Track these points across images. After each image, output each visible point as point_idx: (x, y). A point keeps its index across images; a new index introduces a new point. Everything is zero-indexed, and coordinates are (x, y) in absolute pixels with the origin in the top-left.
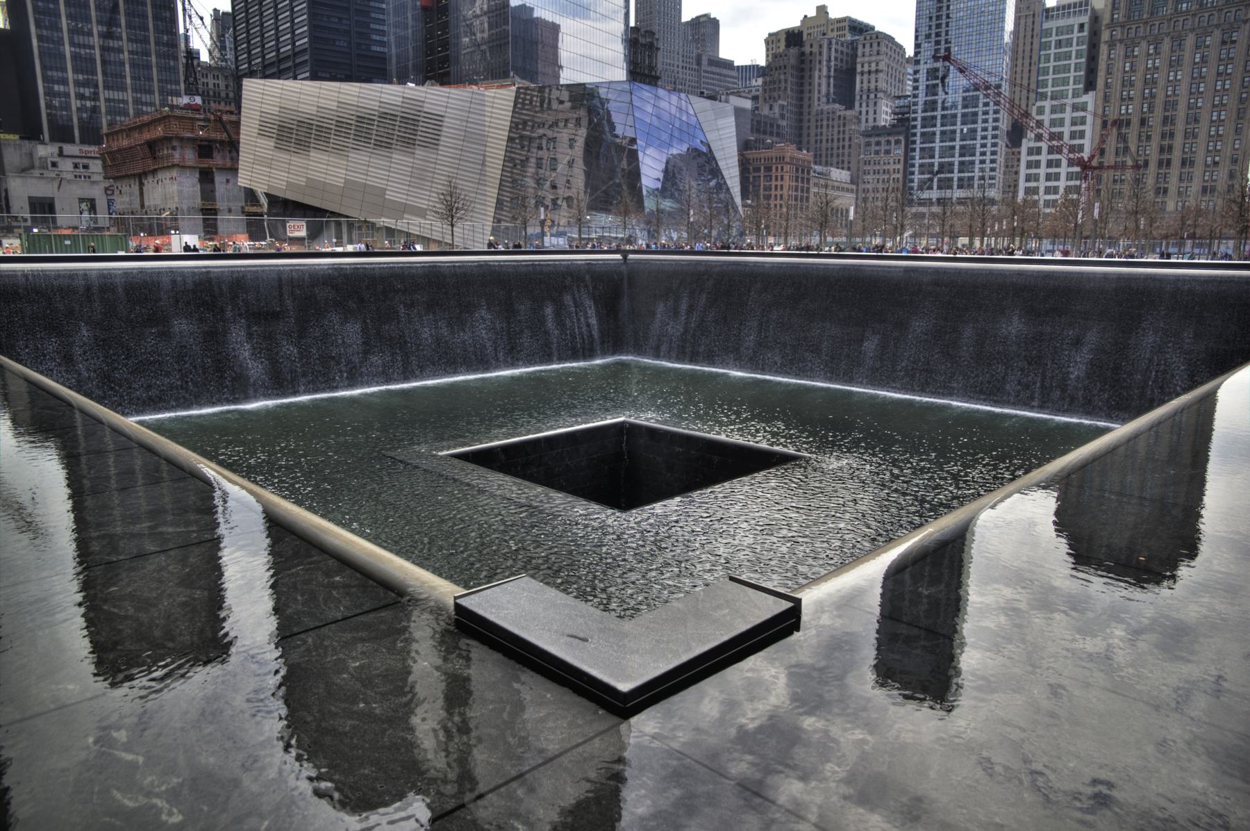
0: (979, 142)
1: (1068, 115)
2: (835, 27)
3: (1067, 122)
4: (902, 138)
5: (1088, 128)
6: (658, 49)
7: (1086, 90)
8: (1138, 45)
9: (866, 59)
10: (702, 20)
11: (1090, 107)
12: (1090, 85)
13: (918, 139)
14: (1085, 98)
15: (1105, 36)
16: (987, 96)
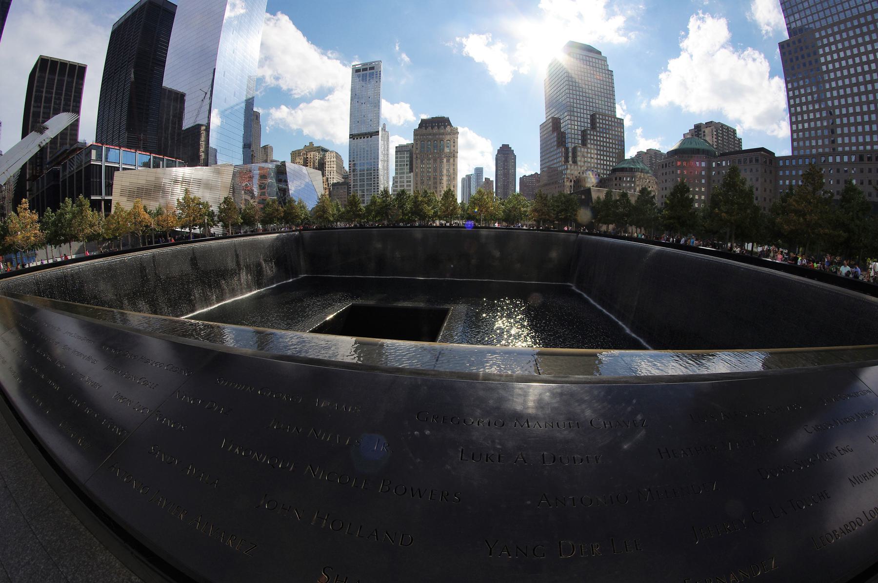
0: (373, 188)
1: (405, 180)
2: (316, 149)
3: (405, 182)
4: (346, 187)
5: (412, 184)
6: (255, 156)
7: (410, 172)
8: (424, 160)
9: (329, 160)
10: (267, 147)
11: (412, 177)
12: (411, 170)
13: (352, 186)
14: (410, 175)
15: (414, 156)
16: (374, 173)
